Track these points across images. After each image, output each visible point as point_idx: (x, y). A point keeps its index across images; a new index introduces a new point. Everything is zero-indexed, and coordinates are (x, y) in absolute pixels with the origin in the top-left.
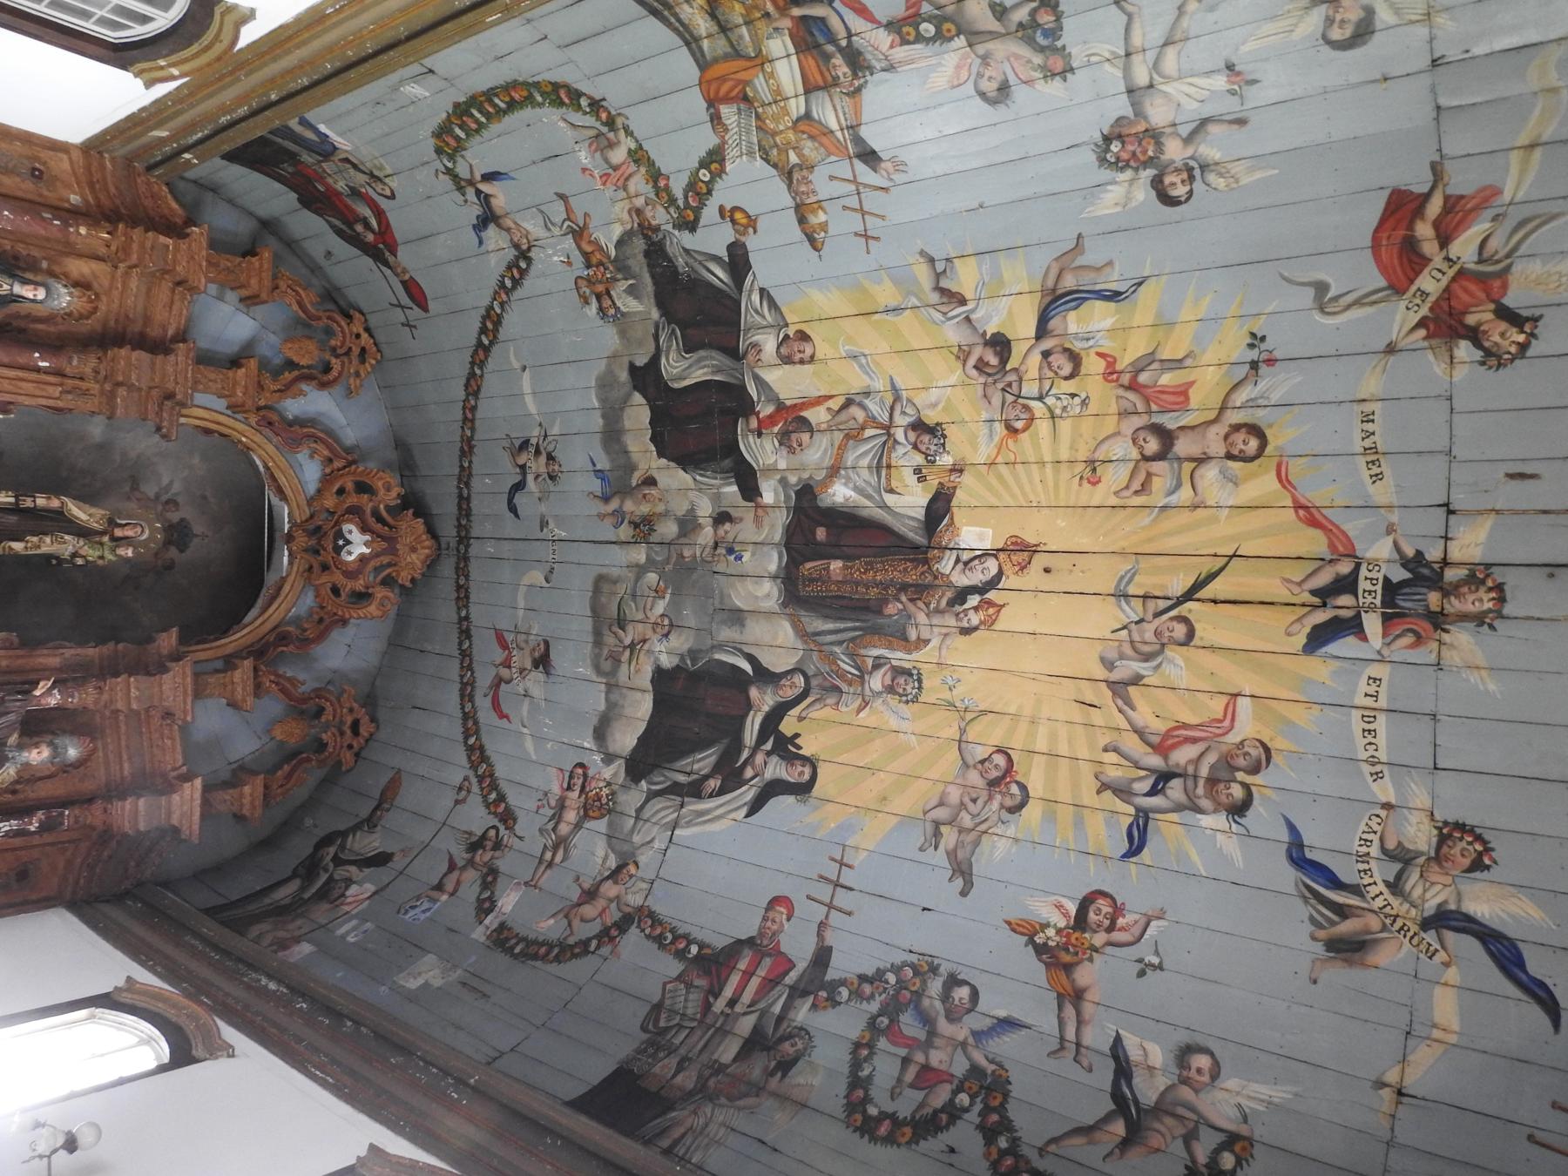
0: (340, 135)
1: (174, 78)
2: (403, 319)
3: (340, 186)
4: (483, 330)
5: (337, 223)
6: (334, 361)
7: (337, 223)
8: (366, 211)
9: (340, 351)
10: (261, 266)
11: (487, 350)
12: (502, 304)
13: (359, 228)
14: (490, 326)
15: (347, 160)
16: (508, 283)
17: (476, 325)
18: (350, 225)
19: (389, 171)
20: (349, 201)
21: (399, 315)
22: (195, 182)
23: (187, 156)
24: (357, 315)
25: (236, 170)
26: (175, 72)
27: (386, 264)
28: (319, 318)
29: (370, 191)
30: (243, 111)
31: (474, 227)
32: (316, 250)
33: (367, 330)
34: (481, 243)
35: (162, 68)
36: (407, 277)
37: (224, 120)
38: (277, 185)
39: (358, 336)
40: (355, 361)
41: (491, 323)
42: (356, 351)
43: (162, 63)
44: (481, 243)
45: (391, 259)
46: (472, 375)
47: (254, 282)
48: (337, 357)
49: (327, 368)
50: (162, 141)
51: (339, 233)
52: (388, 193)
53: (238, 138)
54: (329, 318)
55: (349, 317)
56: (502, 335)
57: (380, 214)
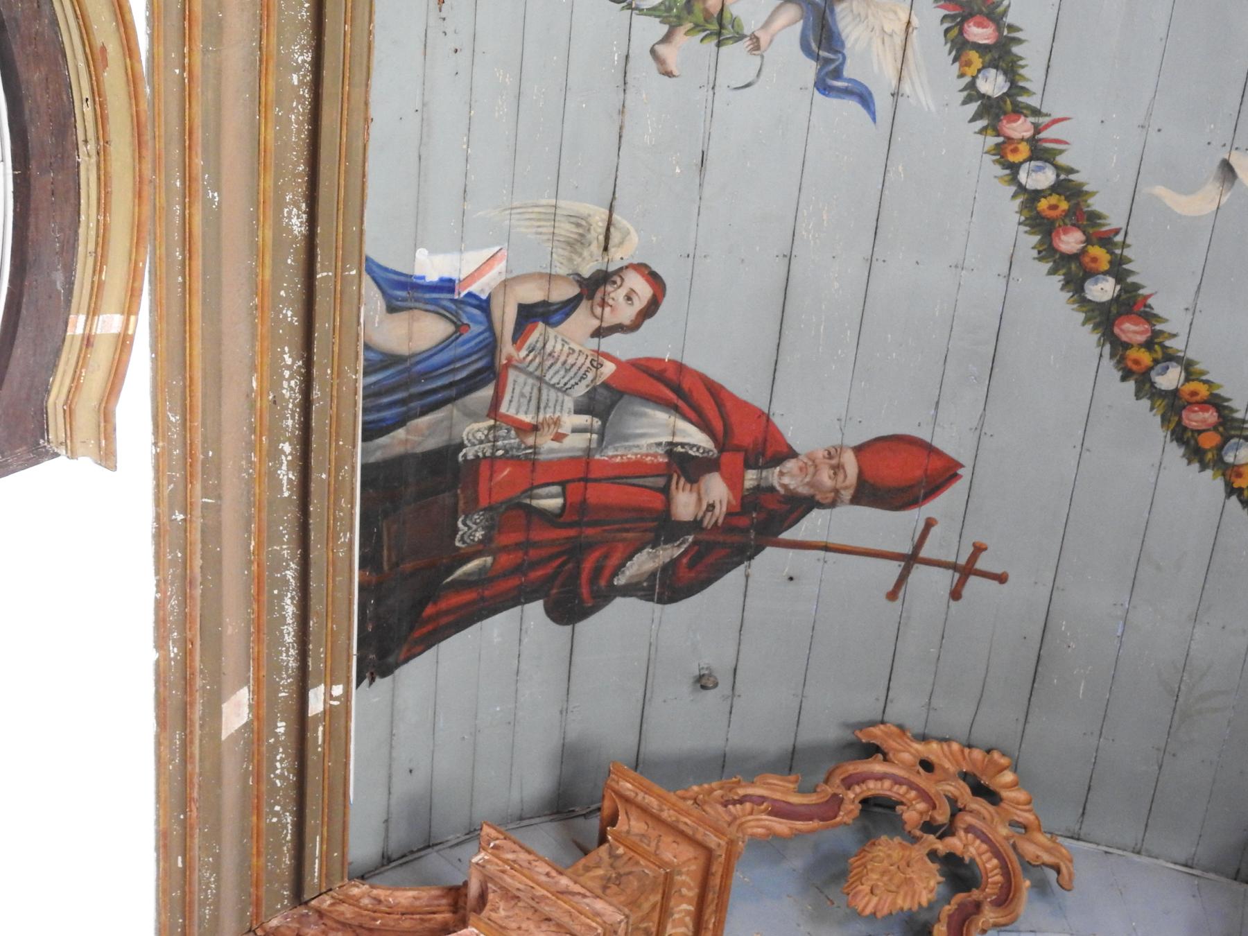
0: (460, 244)
1: (124, 342)
2: (944, 580)
3: (569, 434)
4: (1075, 274)
5: (644, 563)
6: (955, 843)
7: (644, 563)
8: (656, 430)
9: (942, 817)
10: (644, 810)
11: (1131, 302)
12: (1041, 153)
13: (685, 504)
14: (1071, 241)
15: (529, 315)
16: (993, 84)
17: (1048, 288)
18: (664, 527)
19: (599, 217)
20: (614, 453)
21: (930, 583)
22: (386, 860)
23: (316, 703)
24: (877, 730)
25: (416, 673)
26: (109, 323)
27: (799, 505)
28: (836, 802)
29: (624, 347)
30: (290, 388)
31: (822, 86)
32: (685, 726)
33: (924, 738)
34: (865, 98)
35: (88, 341)
36: (850, 462)
37: (286, 475)
38: (497, 627)
39: (927, 765)
40: (979, 805)
41: (1068, 229)
42: (962, 791)
43: (77, 325)
44: (865, 98)
45: (787, 477)
46: (1172, 406)
47: (675, 853)
48: (946, 831)
49: (958, 874)
50: (256, 729)
51: (669, 587)
52: (644, 291)
53: (344, 624)
54: (849, 783)
55: (872, 751)
56: (1114, 219)
57: (673, 386)
